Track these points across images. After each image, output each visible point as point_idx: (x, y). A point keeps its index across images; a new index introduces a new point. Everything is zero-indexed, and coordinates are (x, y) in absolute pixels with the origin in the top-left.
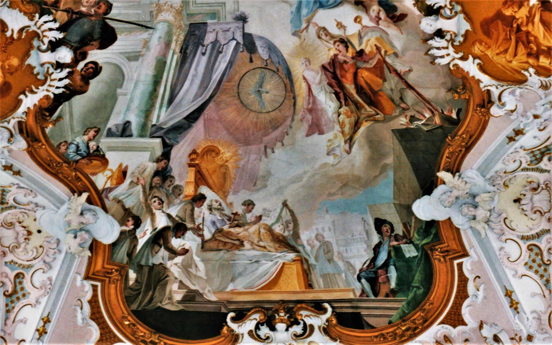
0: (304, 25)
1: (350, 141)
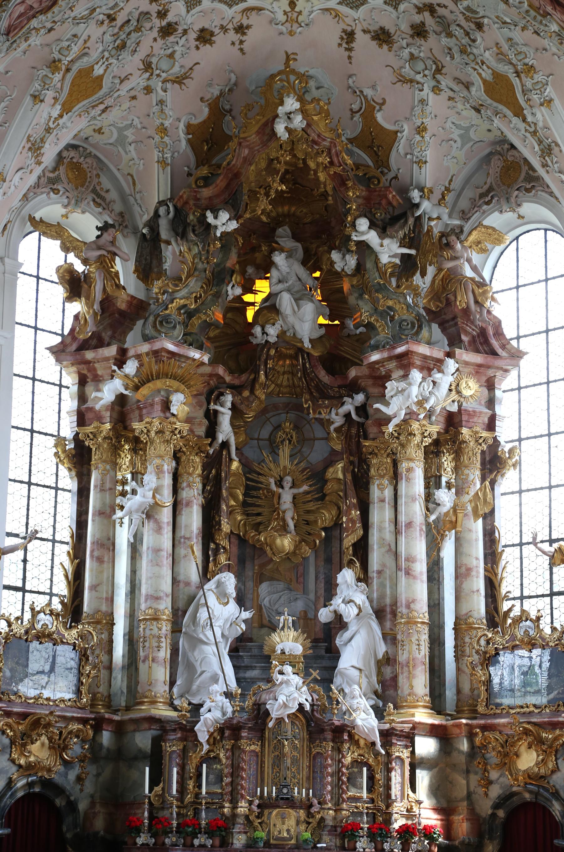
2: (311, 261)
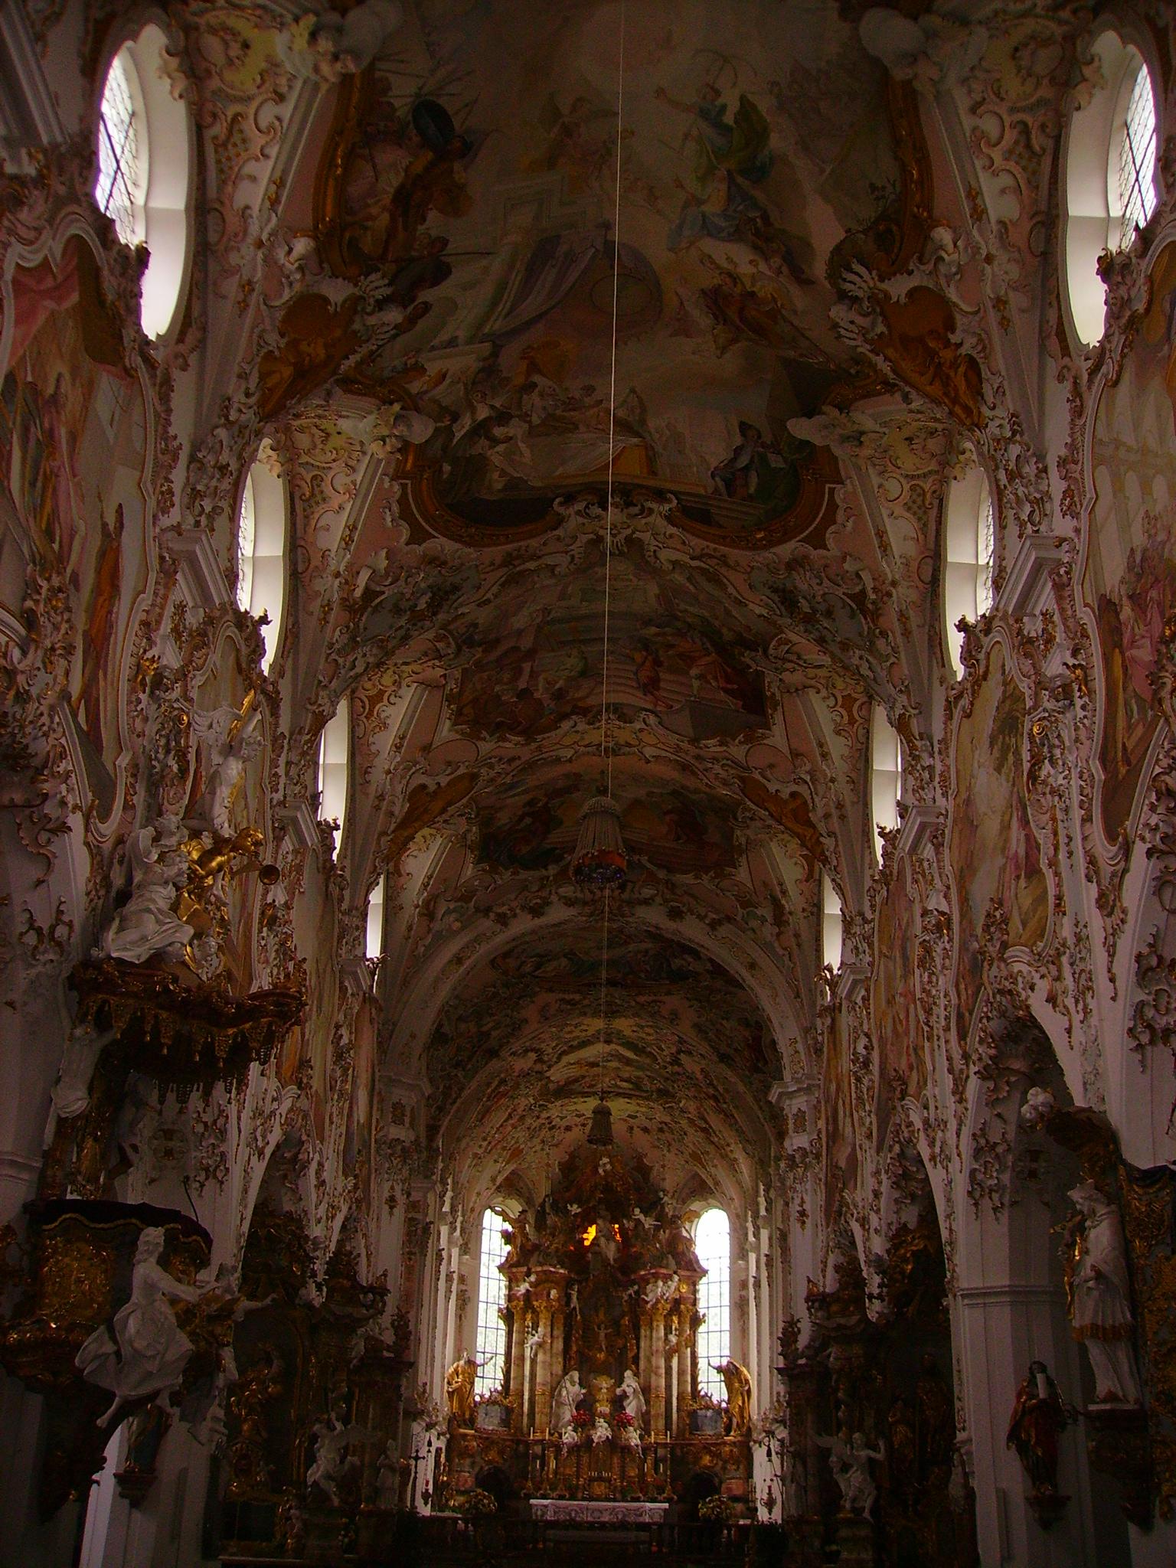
0: (684, 245)
1: (724, 350)
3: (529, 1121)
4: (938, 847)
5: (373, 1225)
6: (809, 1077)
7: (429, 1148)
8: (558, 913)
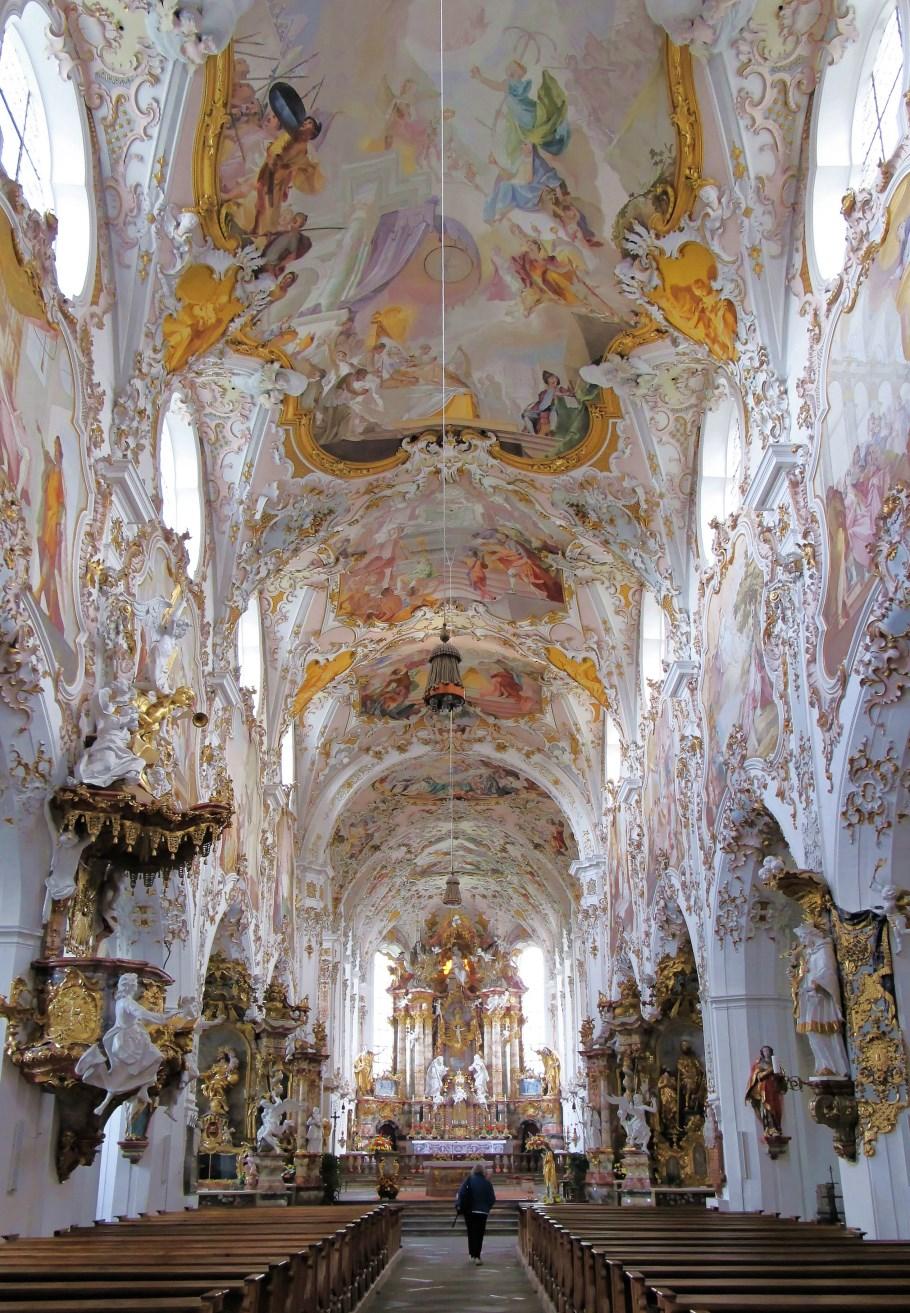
2: (464, 956)
3: (403, 893)
4: (693, 690)
5: (297, 966)
6: (598, 857)
7: (335, 913)
8: (417, 750)
